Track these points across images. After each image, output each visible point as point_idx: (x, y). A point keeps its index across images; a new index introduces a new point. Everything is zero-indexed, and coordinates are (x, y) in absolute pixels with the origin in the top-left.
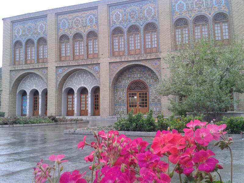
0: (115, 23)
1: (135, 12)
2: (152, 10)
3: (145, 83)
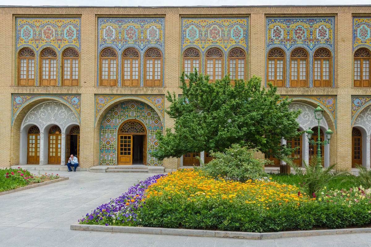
0: (105, 41)
1: (135, 30)
2: (156, 32)
3: (143, 124)
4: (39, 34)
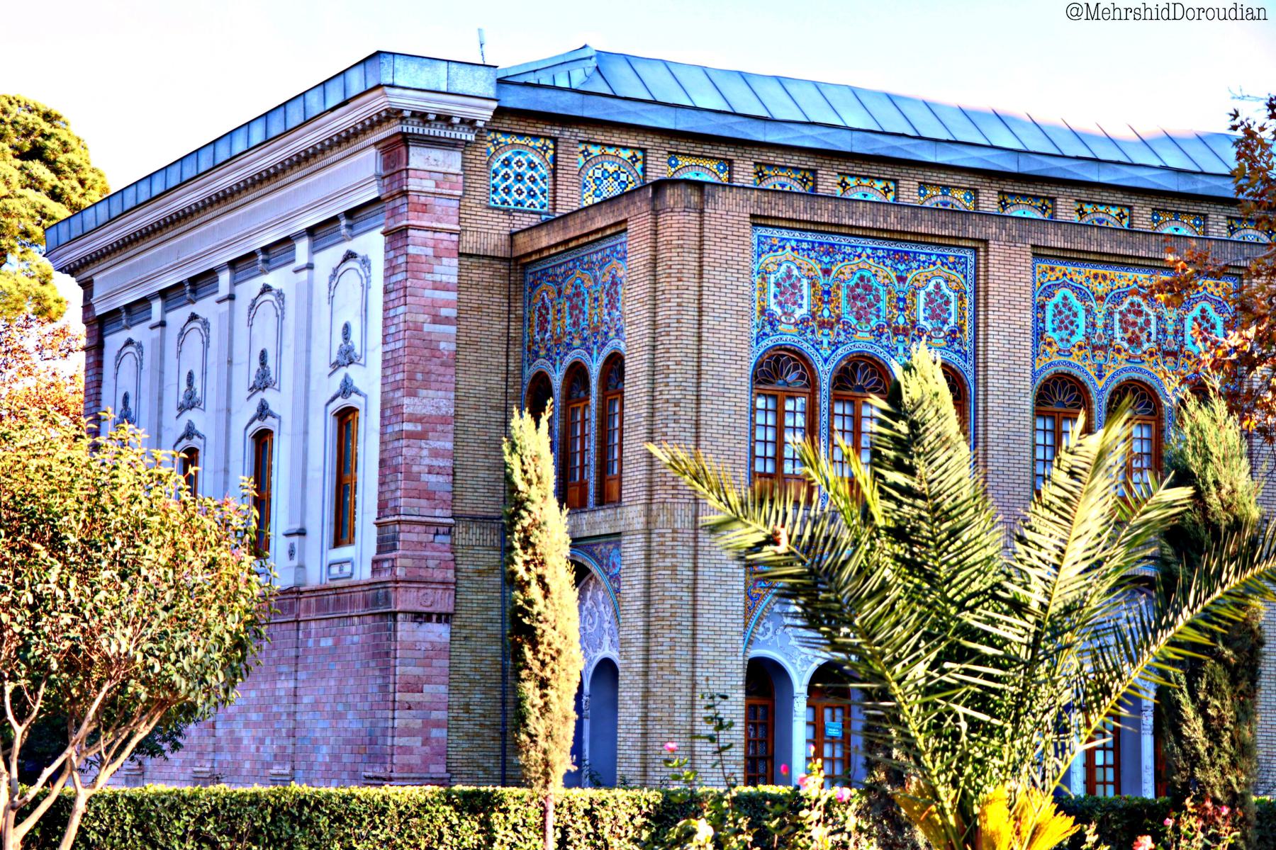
4: (1106, 326)
